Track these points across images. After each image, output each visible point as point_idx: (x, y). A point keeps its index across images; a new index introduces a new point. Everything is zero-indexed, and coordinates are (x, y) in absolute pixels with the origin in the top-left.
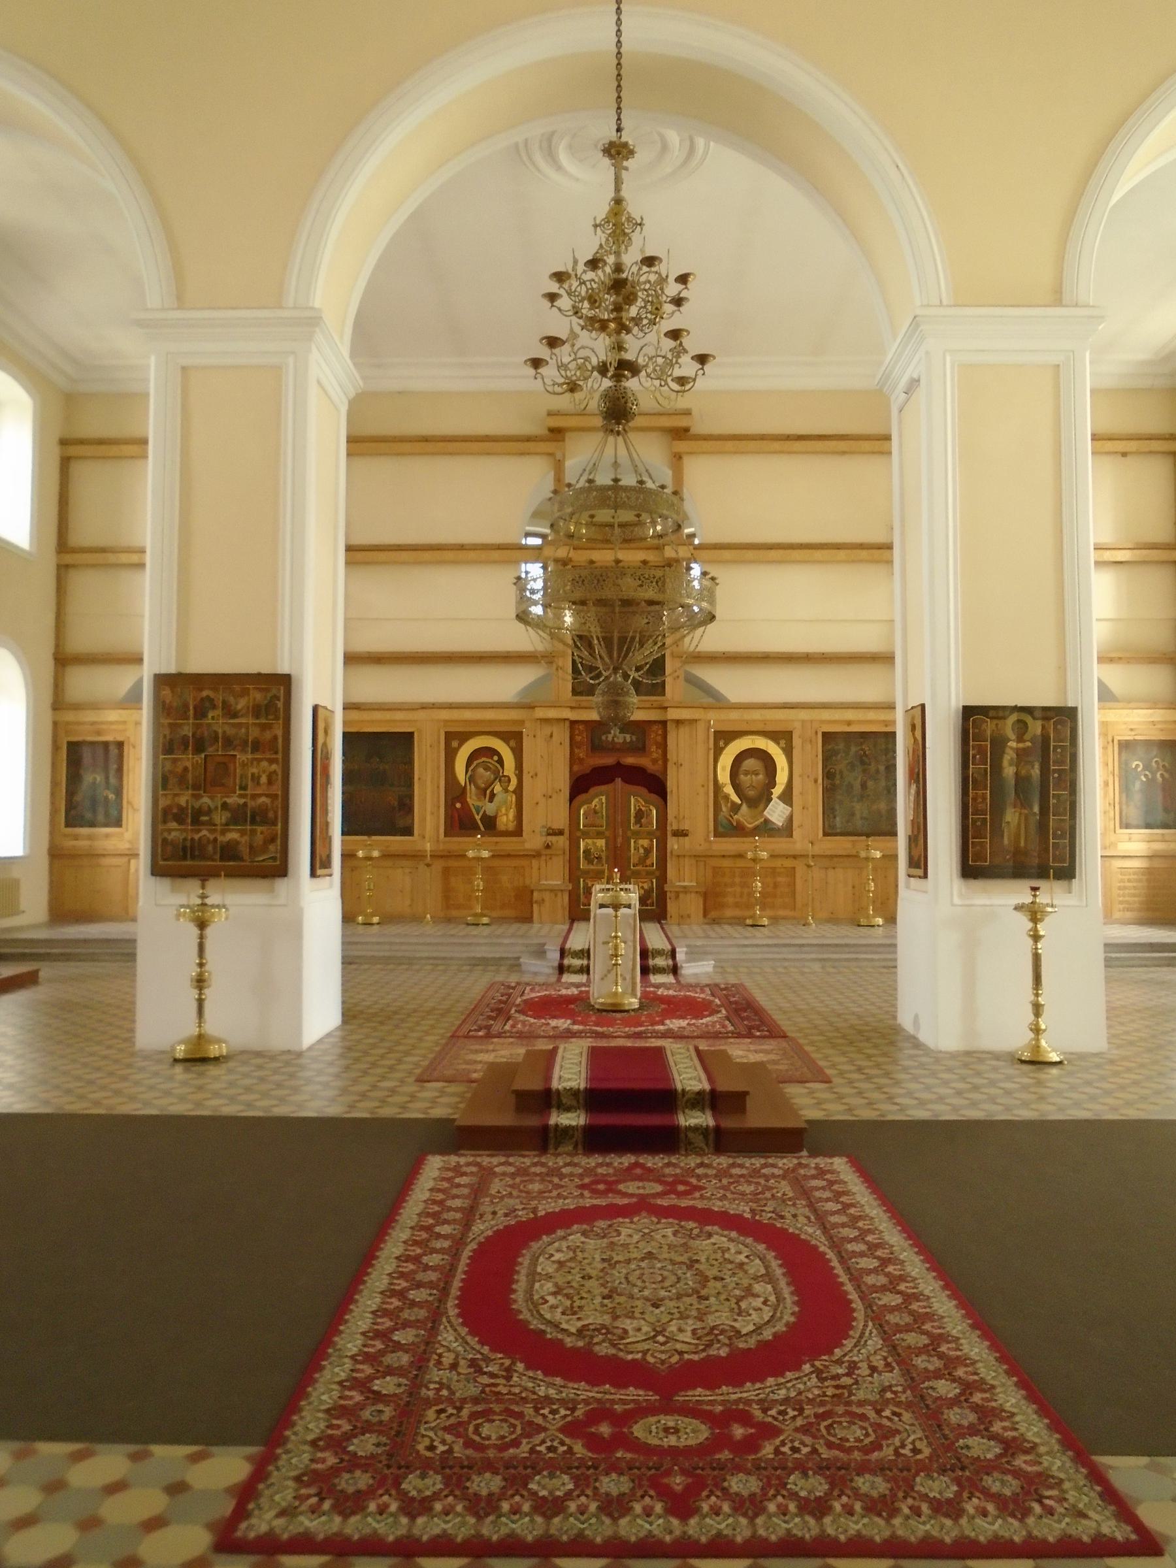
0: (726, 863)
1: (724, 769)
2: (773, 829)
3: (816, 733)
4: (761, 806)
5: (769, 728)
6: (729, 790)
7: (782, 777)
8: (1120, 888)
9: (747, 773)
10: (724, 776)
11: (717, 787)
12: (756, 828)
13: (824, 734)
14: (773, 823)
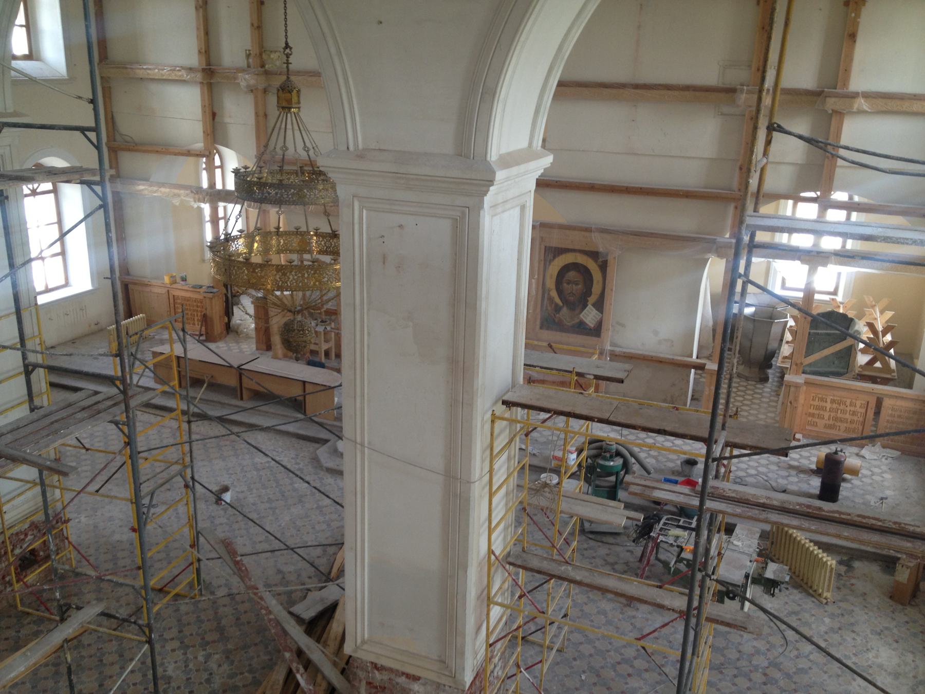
1: (551, 277)
5: (587, 249)
6: (554, 294)
7: (596, 289)
8: (888, 421)
9: (569, 283)
10: (551, 283)
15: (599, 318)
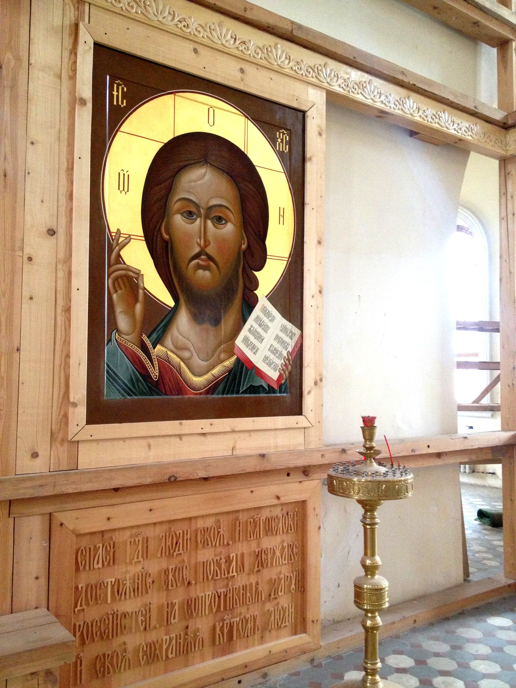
2: (253, 389)
14: (259, 372)
15: (291, 344)
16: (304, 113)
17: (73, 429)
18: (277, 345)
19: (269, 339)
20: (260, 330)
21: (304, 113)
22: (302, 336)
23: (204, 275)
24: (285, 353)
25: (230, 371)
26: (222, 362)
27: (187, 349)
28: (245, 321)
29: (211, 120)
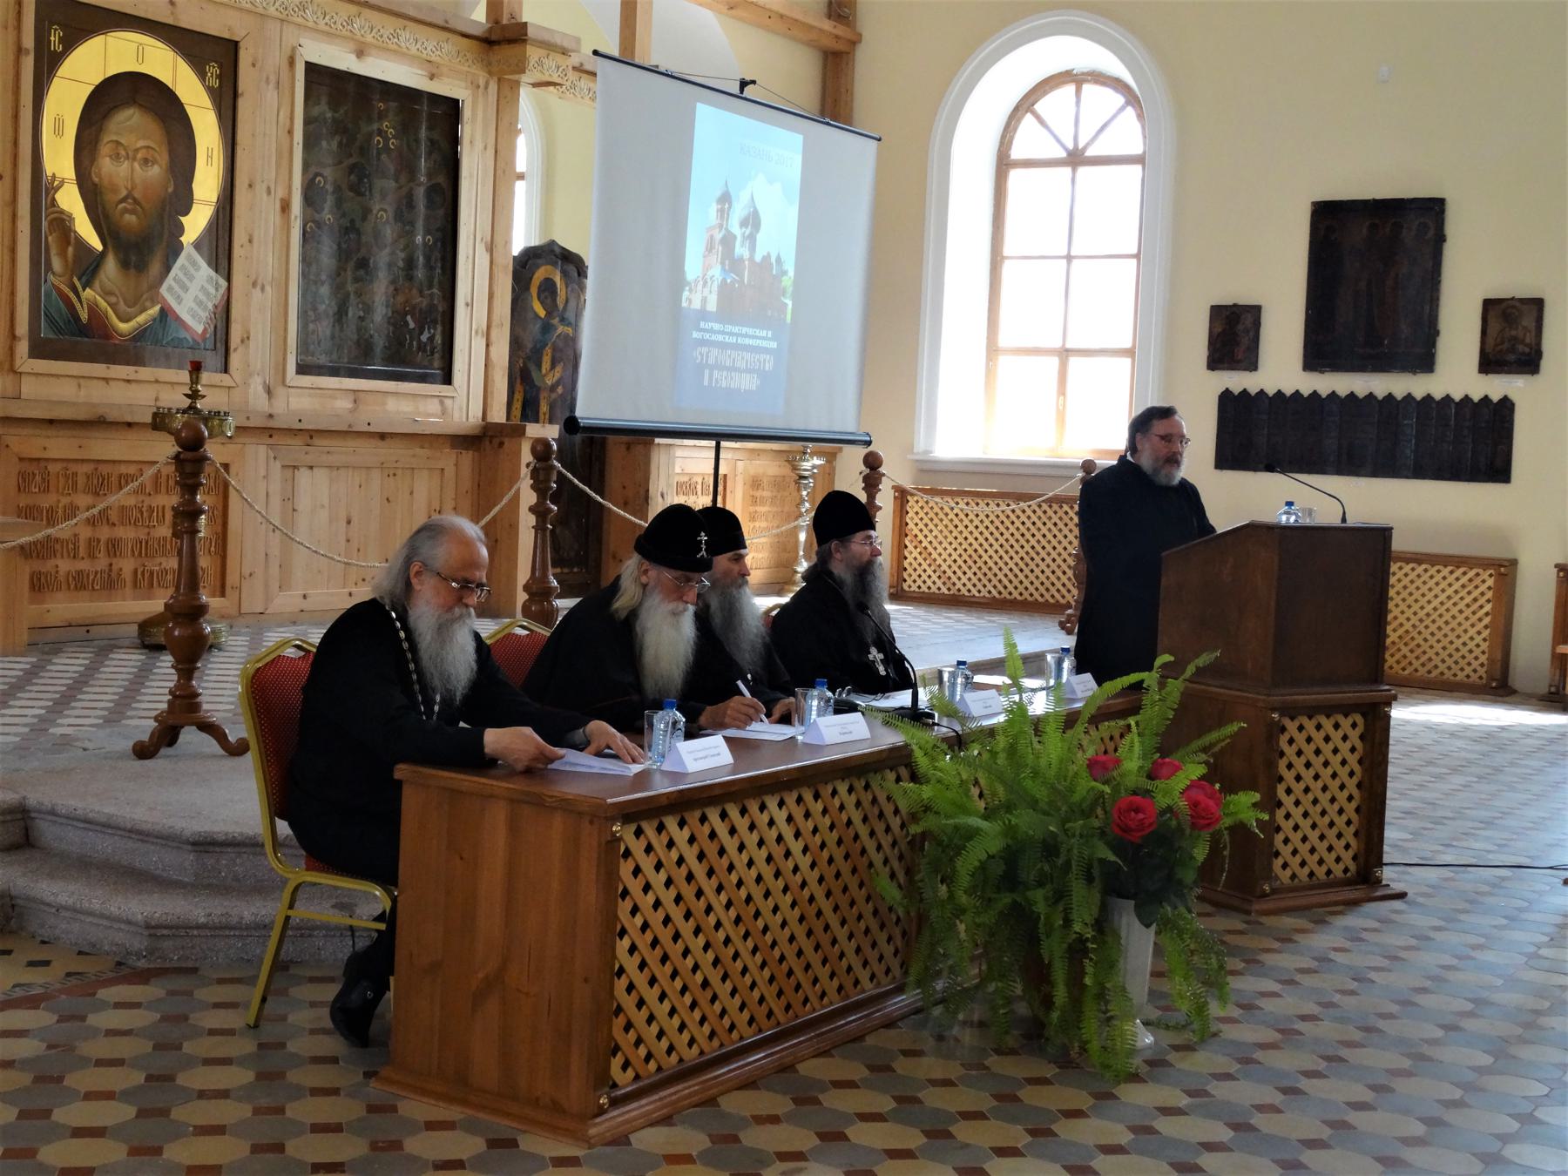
0: (59, 447)
3: (292, 62)
4: (155, 267)
6: (70, 200)
7: (206, 184)
11: (42, 188)
12: (141, 335)
13: (311, 68)
16: (236, 44)
17: (18, 362)
18: (202, 297)
19: (194, 290)
20: (185, 279)
21: (236, 44)
22: (229, 289)
23: (130, 219)
24: (210, 306)
25: (154, 320)
26: (144, 310)
27: (116, 296)
28: (167, 269)
29: (140, 55)
